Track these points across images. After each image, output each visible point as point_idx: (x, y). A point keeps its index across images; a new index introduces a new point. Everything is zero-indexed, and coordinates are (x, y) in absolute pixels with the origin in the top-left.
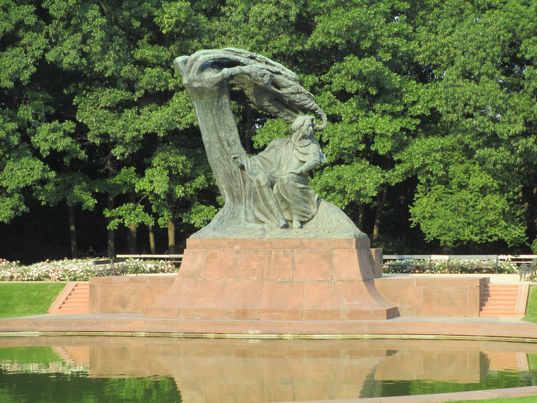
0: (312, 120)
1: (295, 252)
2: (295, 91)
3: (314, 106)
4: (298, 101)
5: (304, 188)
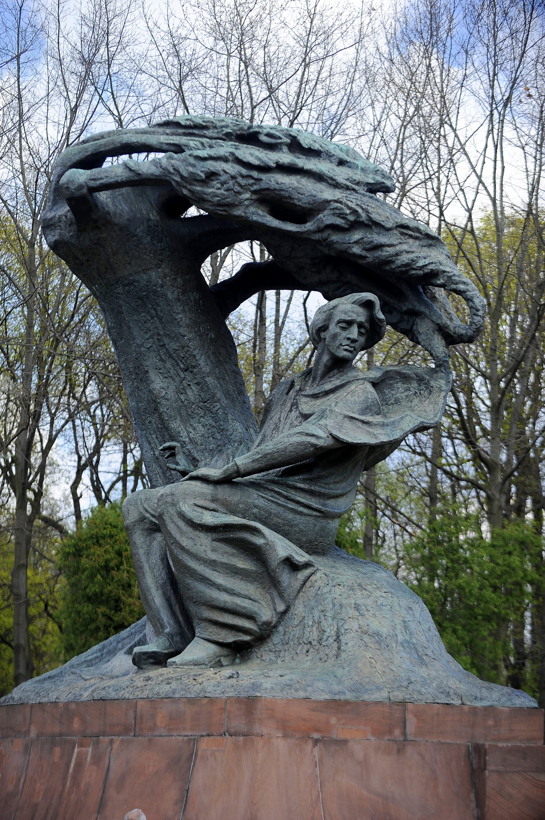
0: (368, 305)
1: (116, 746)
2: (339, 221)
3: (421, 263)
4: (356, 250)
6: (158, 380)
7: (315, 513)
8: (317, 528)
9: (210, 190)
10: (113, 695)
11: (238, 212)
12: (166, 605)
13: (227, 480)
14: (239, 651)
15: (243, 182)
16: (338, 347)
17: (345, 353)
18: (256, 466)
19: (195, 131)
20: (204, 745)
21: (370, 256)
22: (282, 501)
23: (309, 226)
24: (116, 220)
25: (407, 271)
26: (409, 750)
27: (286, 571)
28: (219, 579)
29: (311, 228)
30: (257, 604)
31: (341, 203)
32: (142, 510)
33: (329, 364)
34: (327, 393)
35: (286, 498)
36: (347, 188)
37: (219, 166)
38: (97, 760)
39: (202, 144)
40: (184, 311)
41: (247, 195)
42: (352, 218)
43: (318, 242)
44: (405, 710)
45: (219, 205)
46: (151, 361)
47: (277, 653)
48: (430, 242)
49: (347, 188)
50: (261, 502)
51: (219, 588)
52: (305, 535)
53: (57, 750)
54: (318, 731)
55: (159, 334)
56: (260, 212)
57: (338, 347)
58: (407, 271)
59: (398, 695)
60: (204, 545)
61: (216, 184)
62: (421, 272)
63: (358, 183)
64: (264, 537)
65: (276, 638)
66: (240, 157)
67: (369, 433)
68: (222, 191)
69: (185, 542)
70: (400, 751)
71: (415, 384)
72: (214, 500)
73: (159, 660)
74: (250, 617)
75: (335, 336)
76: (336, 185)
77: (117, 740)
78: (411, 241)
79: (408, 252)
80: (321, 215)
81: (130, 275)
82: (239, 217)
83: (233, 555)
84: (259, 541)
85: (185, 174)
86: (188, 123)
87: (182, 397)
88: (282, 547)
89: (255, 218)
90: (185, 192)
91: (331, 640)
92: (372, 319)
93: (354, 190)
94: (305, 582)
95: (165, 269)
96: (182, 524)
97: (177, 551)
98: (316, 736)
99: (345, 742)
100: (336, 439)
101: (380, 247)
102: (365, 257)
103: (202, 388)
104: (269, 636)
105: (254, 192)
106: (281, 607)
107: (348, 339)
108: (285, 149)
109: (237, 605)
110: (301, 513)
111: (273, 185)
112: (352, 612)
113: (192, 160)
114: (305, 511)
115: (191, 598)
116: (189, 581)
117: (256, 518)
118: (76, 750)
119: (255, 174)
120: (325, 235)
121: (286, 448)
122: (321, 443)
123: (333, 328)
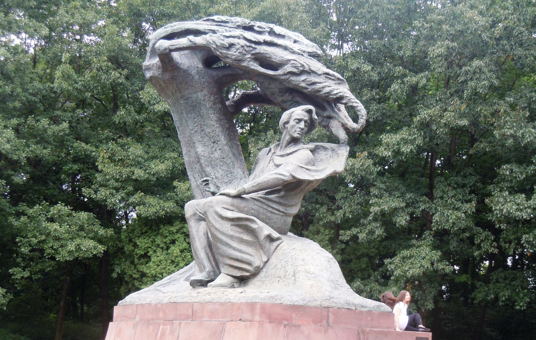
0: (309, 112)
1: (182, 325)
2: (295, 70)
3: (335, 92)
4: (303, 85)
5: (239, 219)
6: (200, 147)
7: (281, 214)
8: (282, 221)
9: (231, 53)
10: (180, 300)
11: (245, 64)
12: (206, 257)
13: (238, 196)
14: (242, 281)
15: (247, 49)
16: (294, 132)
17: (298, 135)
18: (254, 189)
19: (221, 24)
20: (229, 325)
21: (310, 88)
22: (265, 207)
23: (280, 72)
24: (182, 67)
25: (328, 96)
26: (330, 331)
27: (268, 241)
28: (235, 244)
29: (281, 73)
30: (253, 258)
31: (296, 61)
32: (195, 210)
33: (289, 140)
34: (288, 154)
35: (267, 205)
36: (299, 54)
37: (235, 41)
38: (172, 332)
39: (226, 30)
40: (214, 113)
41: (249, 56)
42: (301, 69)
43: (284, 80)
44: (328, 311)
45: (235, 60)
46: (197, 138)
47: (263, 282)
48: (340, 82)
49: (299, 54)
50: (255, 207)
51: (234, 249)
52: (276, 225)
53: (151, 327)
54: (286, 320)
55: (201, 125)
56: (255, 64)
57: (294, 132)
58: (328, 96)
59: (326, 304)
60: (227, 228)
61: (233, 49)
62: (335, 97)
63: (304, 52)
64: (257, 224)
65: (262, 274)
66: (246, 37)
67: (309, 174)
68: (237, 53)
69: (217, 226)
70: (326, 331)
71: (330, 152)
72: (232, 205)
73: (203, 284)
74: (249, 264)
75: (293, 127)
76: (294, 52)
77: (183, 323)
78: (330, 81)
79: (329, 86)
80: (285, 67)
81: (188, 94)
82: (244, 66)
83: (241, 233)
84: (254, 226)
85: (218, 44)
86: (218, 20)
87: (212, 156)
88: (266, 230)
89: (252, 67)
90: (218, 53)
91: (291, 276)
92: (311, 119)
93: (302, 55)
94: (277, 247)
95: (205, 92)
96: (216, 217)
97: (213, 230)
98: (285, 323)
99: (299, 326)
100: (294, 177)
101: (314, 83)
102: (307, 88)
103: (222, 152)
104: (258, 273)
105: (253, 54)
106: (265, 259)
107: (300, 128)
108: (267, 34)
109: (243, 257)
110: (275, 213)
111: (262, 51)
112: (301, 263)
113: (222, 38)
114: (277, 212)
115: (220, 254)
116: (219, 245)
117: (253, 215)
118: (161, 327)
119: (253, 45)
120: (287, 76)
121: (269, 180)
122: (286, 178)
123: (292, 123)
